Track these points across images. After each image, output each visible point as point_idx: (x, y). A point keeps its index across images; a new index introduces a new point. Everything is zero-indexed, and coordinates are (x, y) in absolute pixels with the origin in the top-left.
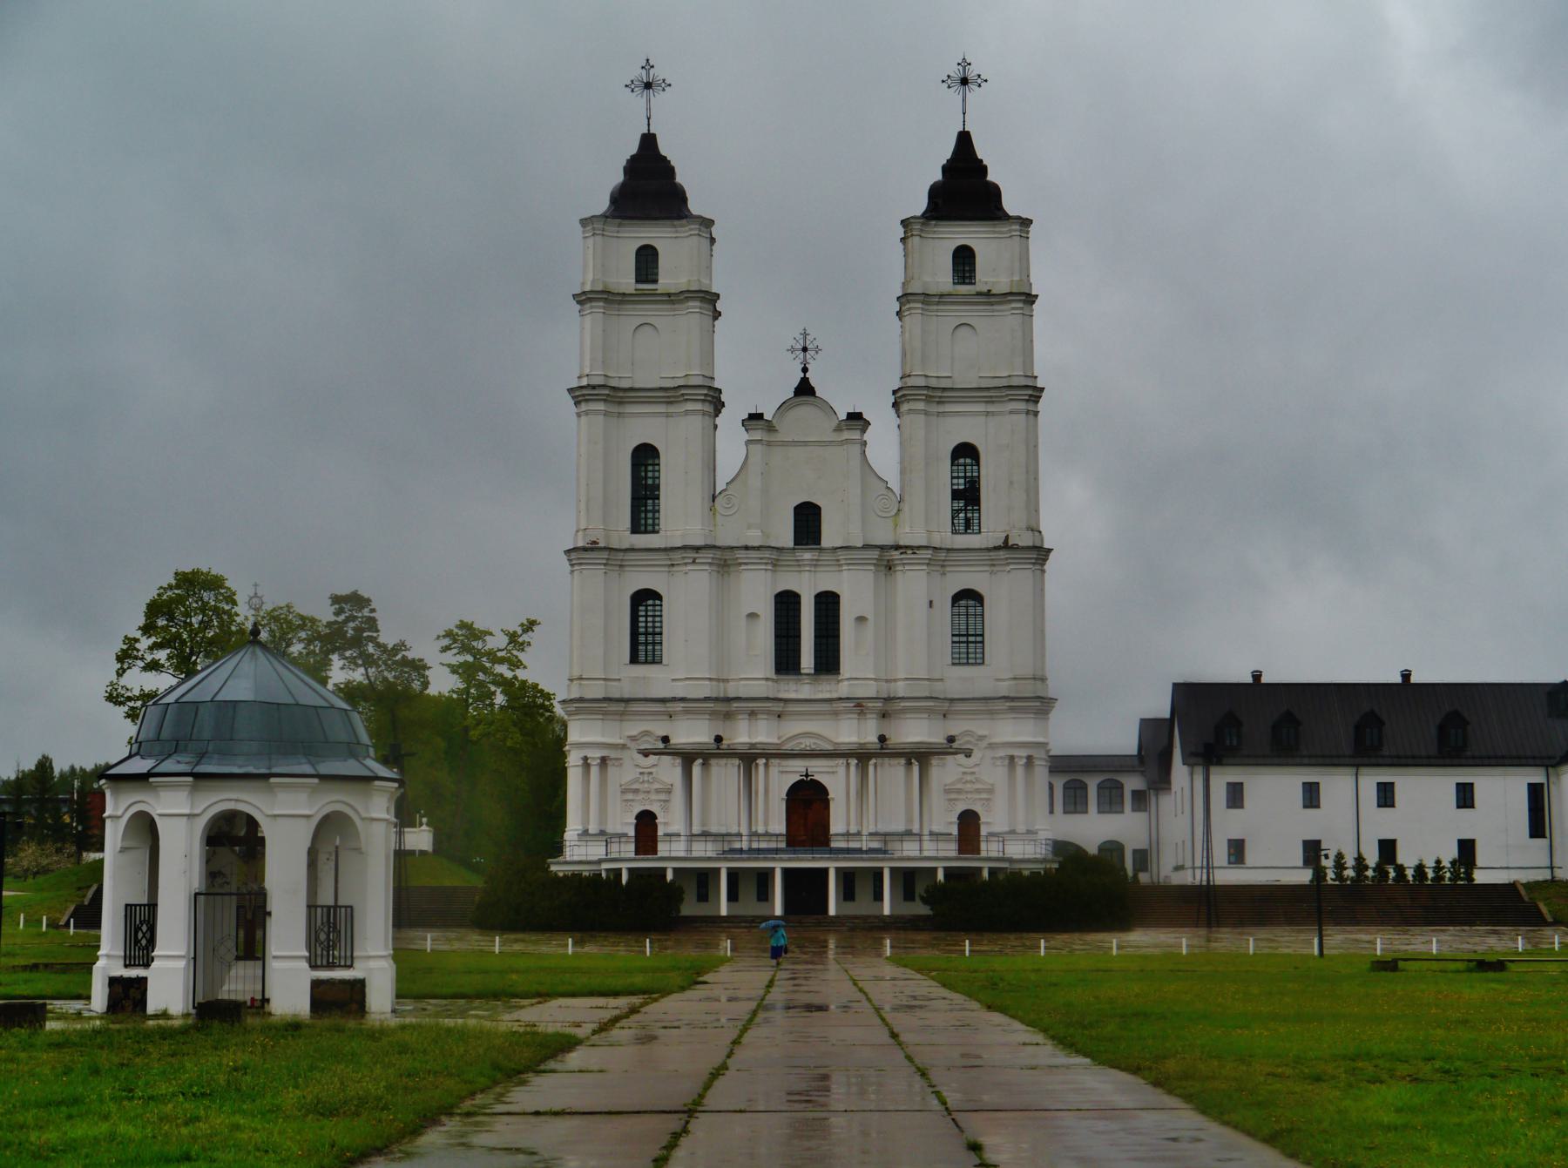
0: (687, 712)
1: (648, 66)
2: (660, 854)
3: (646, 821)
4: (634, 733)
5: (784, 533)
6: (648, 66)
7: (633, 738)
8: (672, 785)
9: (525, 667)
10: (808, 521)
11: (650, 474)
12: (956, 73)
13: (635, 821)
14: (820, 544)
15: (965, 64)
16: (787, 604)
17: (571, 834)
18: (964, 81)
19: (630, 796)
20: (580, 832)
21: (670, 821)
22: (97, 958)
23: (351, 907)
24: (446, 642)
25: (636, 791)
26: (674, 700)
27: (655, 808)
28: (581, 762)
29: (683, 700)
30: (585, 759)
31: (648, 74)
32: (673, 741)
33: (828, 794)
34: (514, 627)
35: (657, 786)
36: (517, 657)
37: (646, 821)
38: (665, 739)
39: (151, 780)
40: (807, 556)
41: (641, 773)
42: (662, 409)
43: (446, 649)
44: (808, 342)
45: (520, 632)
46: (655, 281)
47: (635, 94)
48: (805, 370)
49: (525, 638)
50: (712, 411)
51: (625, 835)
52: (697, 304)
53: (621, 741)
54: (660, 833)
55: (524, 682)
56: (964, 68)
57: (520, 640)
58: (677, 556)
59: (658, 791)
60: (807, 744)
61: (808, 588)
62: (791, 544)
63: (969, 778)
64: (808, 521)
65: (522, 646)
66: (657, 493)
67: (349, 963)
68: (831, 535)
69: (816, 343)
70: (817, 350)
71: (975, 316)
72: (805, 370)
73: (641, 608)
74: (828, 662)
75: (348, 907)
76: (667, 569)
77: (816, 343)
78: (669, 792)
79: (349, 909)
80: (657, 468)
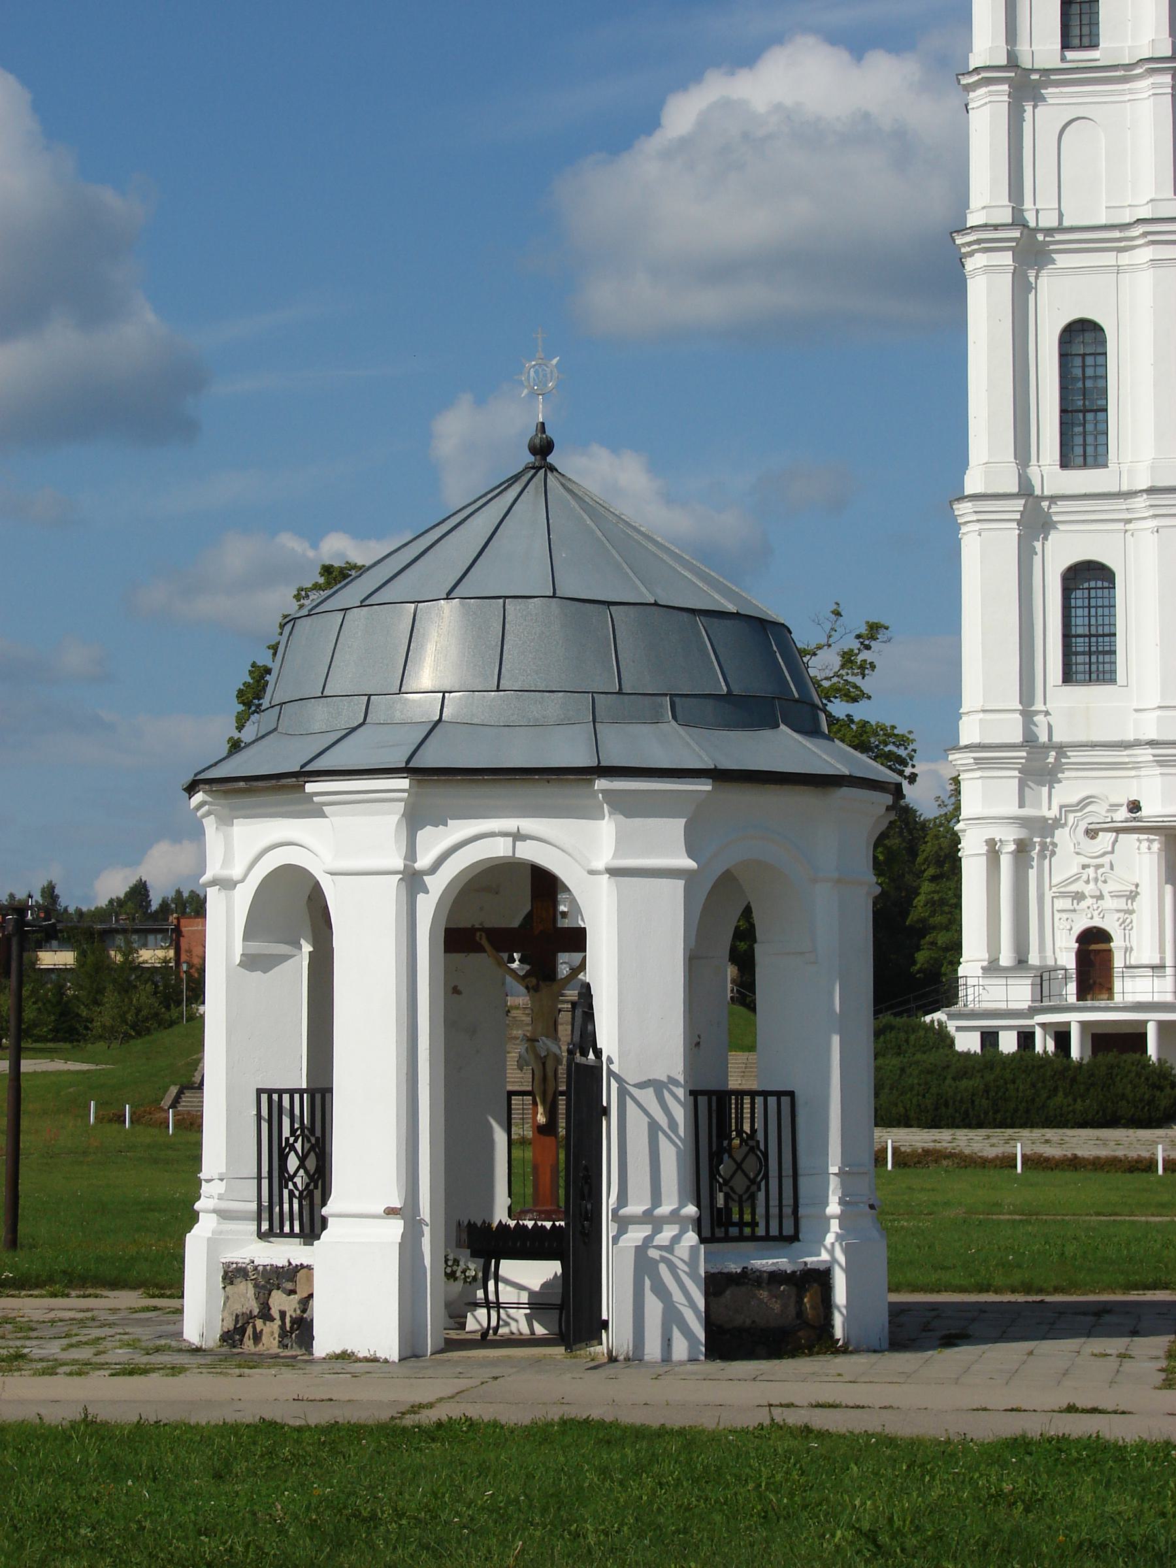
0: (1161, 762)
2: (1118, 998)
8: (1137, 886)
9: (869, 698)
11: (1090, 372)
13: (1077, 945)
17: (970, 966)
20: (985, 964)
22: (194, 1218)
23: (791, 1094)
25: (1079, 897)
26: (1137, 744)
27: (1109, 924)
28: (984, 849)
29: (1152, 743)
30: (991, 843)
32: (1145, 812)
34: (863, 630)
36: (856, 687)
38: (1135, 807)
39: (310, 787)
41: (1084, 867)
42: (1108, 258)
45: (855, 645)
46: (1094, 46)
49: (865, 655)
54: (1118, 962)
55: (864, 724)
57: (860, 658)
58: (1141, 502)
59: (1115, 896)
65: (865, 668)
66: (1103, 402)
67: (788, 1230)
73: (1079, 593)
75: (779, 1094)
76: (1121, 526)
78: (1132, 896)
79: (785, 1100)
80: (1100, 359)
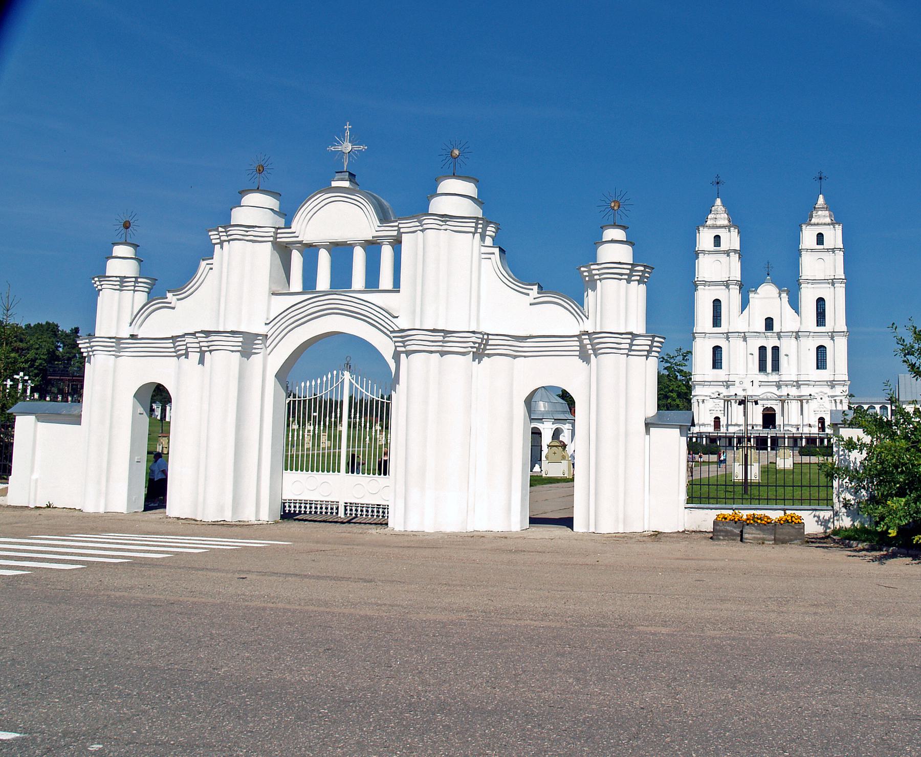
1: (718, 177)
3: (717, 420)
5: (761, 327)
6: (718, 177)
10: (769, 323)
12: (818, 176)
14: (773, 330)
15: (821, 173)
16: (762, 349)
18: (821, 178)
19: (712, 412)
21: (723, 421)
24: (661, 360)
25: (714, 410)
31: (718, 179)
33: (775, 411)
37: (717, 420)
40: (769, 334)
43: (662, 361)
50: (738, 288)
51: (710, 424)
52: (733, 253)
60: (769, 395)
61: (770, 344)
62: (764, 331)
63: (822, 406)
64: (769, 323)
68: (776, 328)
70: (772, 267)
71: (825, 255)
74: (776, 367)
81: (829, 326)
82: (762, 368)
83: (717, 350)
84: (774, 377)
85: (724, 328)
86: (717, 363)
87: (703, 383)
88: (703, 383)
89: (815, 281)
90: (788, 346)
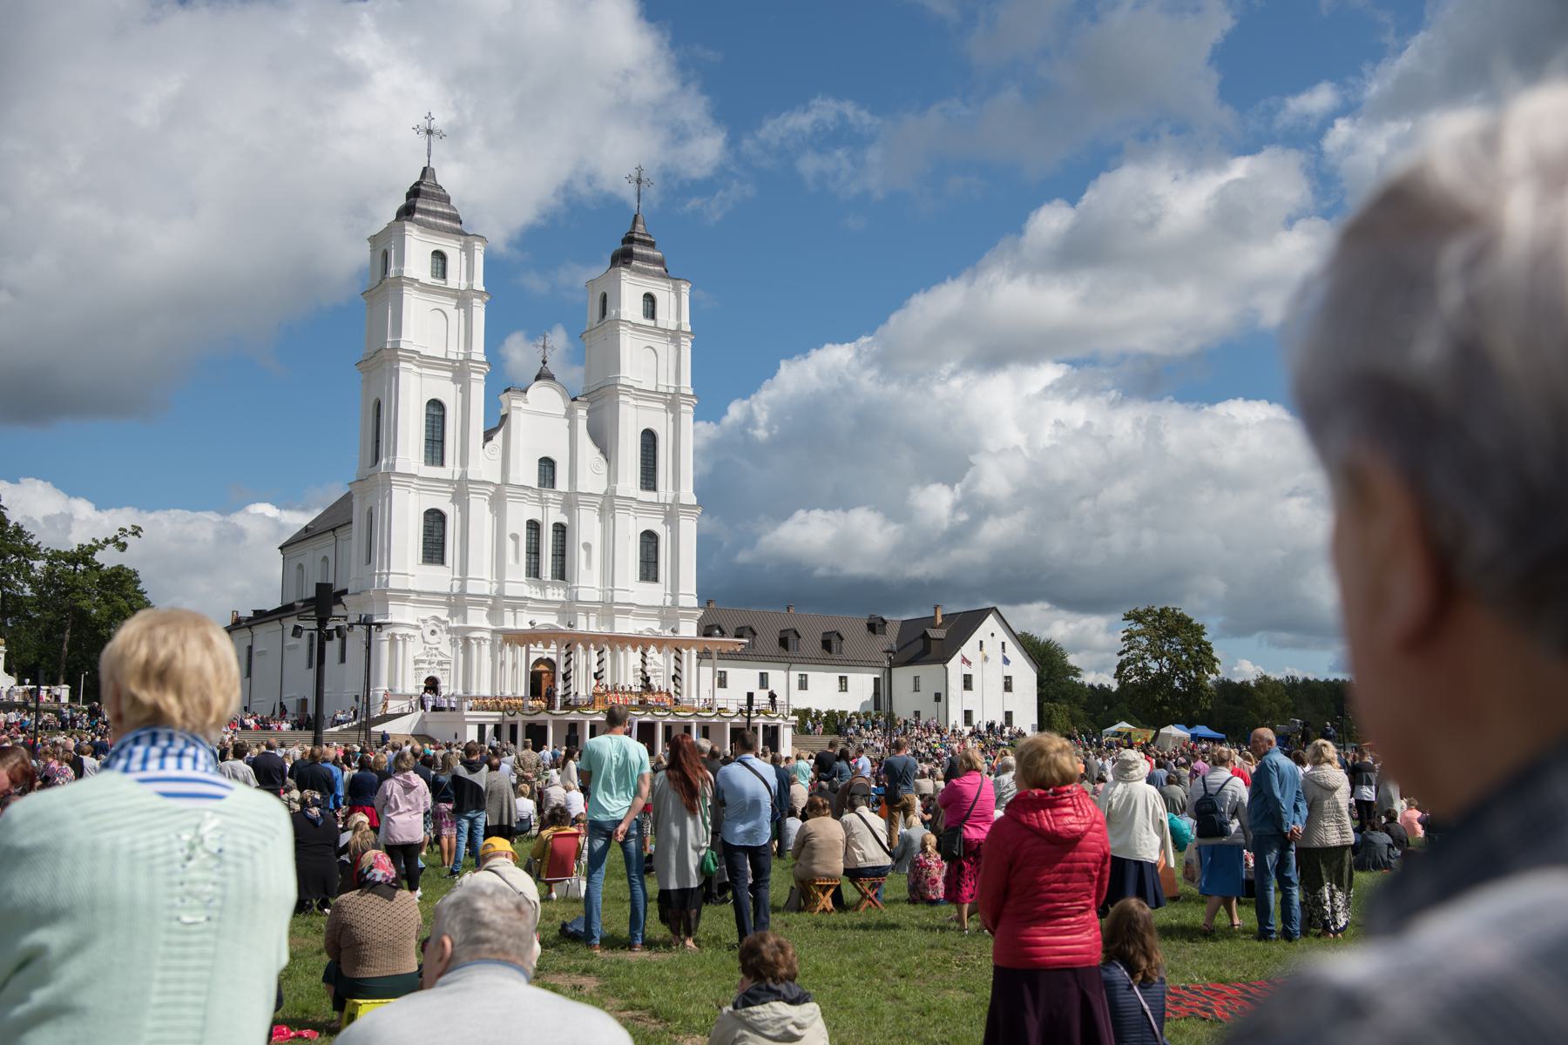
4: (424, 617)
5: (533, 480)
7: (424, 621)
12: (635, 175)
16: (534, 527)
19: (421, 665)
25: (423, 661)
35: (441, 658)
44: (547, 342)
47: (419, 136)
48: (544, 362)
53: (417, 623)
56: (640, 172)
59: (440, 663)
62: (535, 486)
69: (552, 344)
72: (544, 362)
74: (561, 573)
77: (552, 344)
81: (664, 491)
82: (534, 571)
83: (434, 520)
84: (556, 594)
85: (451, 469)
86: (434, 550)
87: (403, 596)
88: (403, 596)
89: (642, 394)
90: (588, 527)
